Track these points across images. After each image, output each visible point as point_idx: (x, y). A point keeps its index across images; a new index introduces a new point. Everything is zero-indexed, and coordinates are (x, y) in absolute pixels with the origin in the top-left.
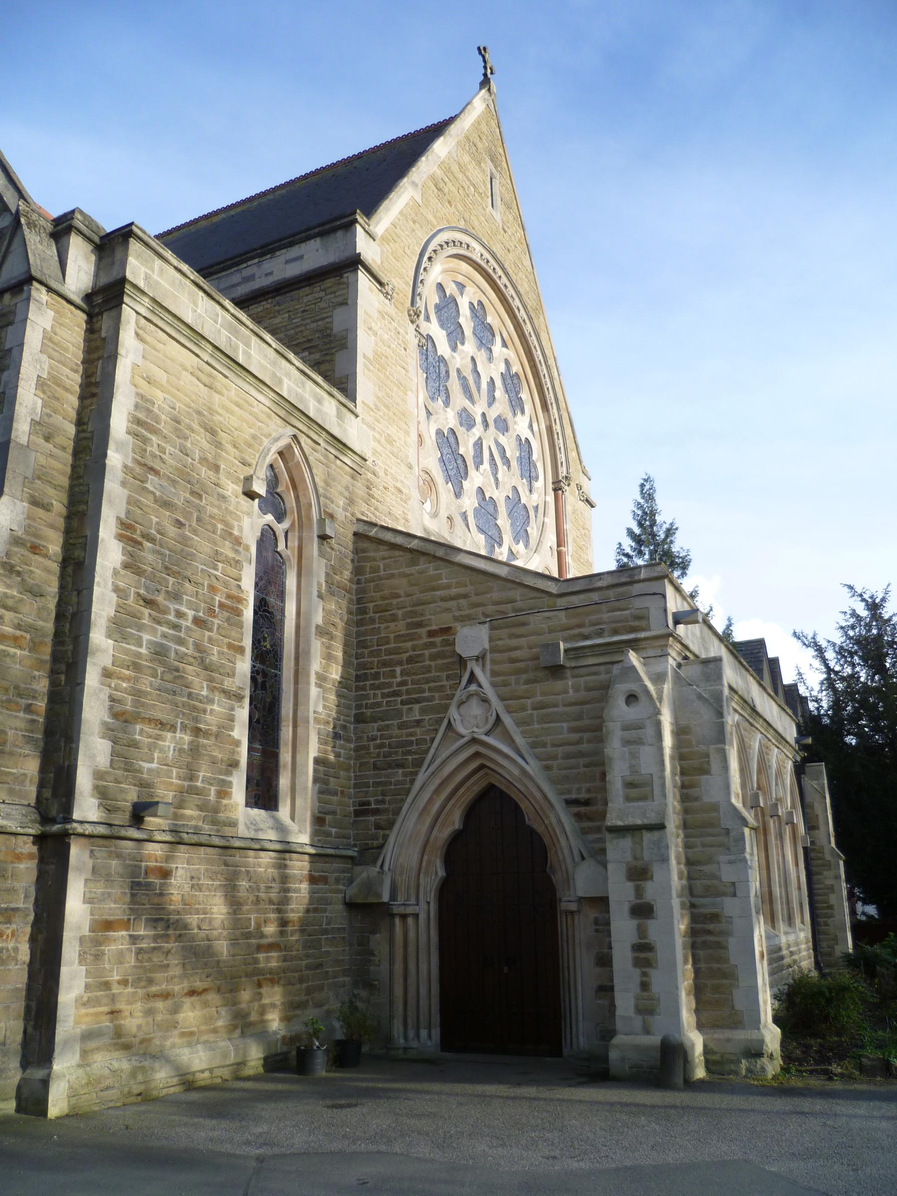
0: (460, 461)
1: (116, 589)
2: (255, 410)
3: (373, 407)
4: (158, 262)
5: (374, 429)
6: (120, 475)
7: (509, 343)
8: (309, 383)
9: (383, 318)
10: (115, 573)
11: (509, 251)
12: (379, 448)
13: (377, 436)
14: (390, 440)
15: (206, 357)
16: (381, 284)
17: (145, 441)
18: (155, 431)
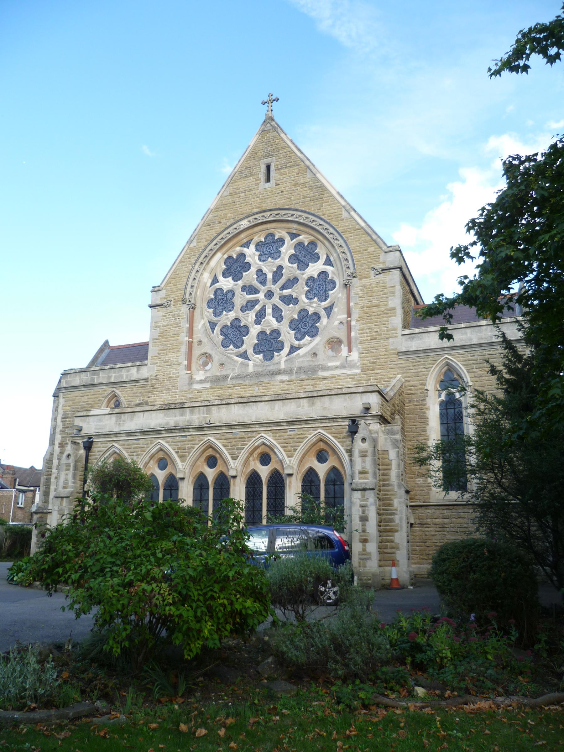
0: (244, 329)
1: (58, 459)
2: (100, 392)
3: (157, 355)
4: (69, 375)
5: (157, 363)
6: (59, 433)
7: (299, 233)
8: (123, 370)
9: (165, 316)
10: (58, 456)
11: (282, 192)
12: (160, 368)
13: (159, 364)
14: (166, 361)
15: (83, 389)
16: (162, 305)
17: (65, 421)
18: (67, 418)
